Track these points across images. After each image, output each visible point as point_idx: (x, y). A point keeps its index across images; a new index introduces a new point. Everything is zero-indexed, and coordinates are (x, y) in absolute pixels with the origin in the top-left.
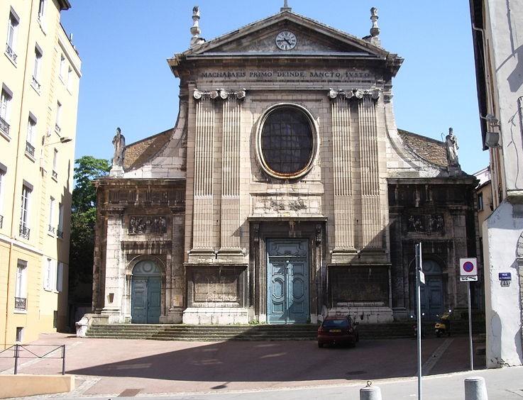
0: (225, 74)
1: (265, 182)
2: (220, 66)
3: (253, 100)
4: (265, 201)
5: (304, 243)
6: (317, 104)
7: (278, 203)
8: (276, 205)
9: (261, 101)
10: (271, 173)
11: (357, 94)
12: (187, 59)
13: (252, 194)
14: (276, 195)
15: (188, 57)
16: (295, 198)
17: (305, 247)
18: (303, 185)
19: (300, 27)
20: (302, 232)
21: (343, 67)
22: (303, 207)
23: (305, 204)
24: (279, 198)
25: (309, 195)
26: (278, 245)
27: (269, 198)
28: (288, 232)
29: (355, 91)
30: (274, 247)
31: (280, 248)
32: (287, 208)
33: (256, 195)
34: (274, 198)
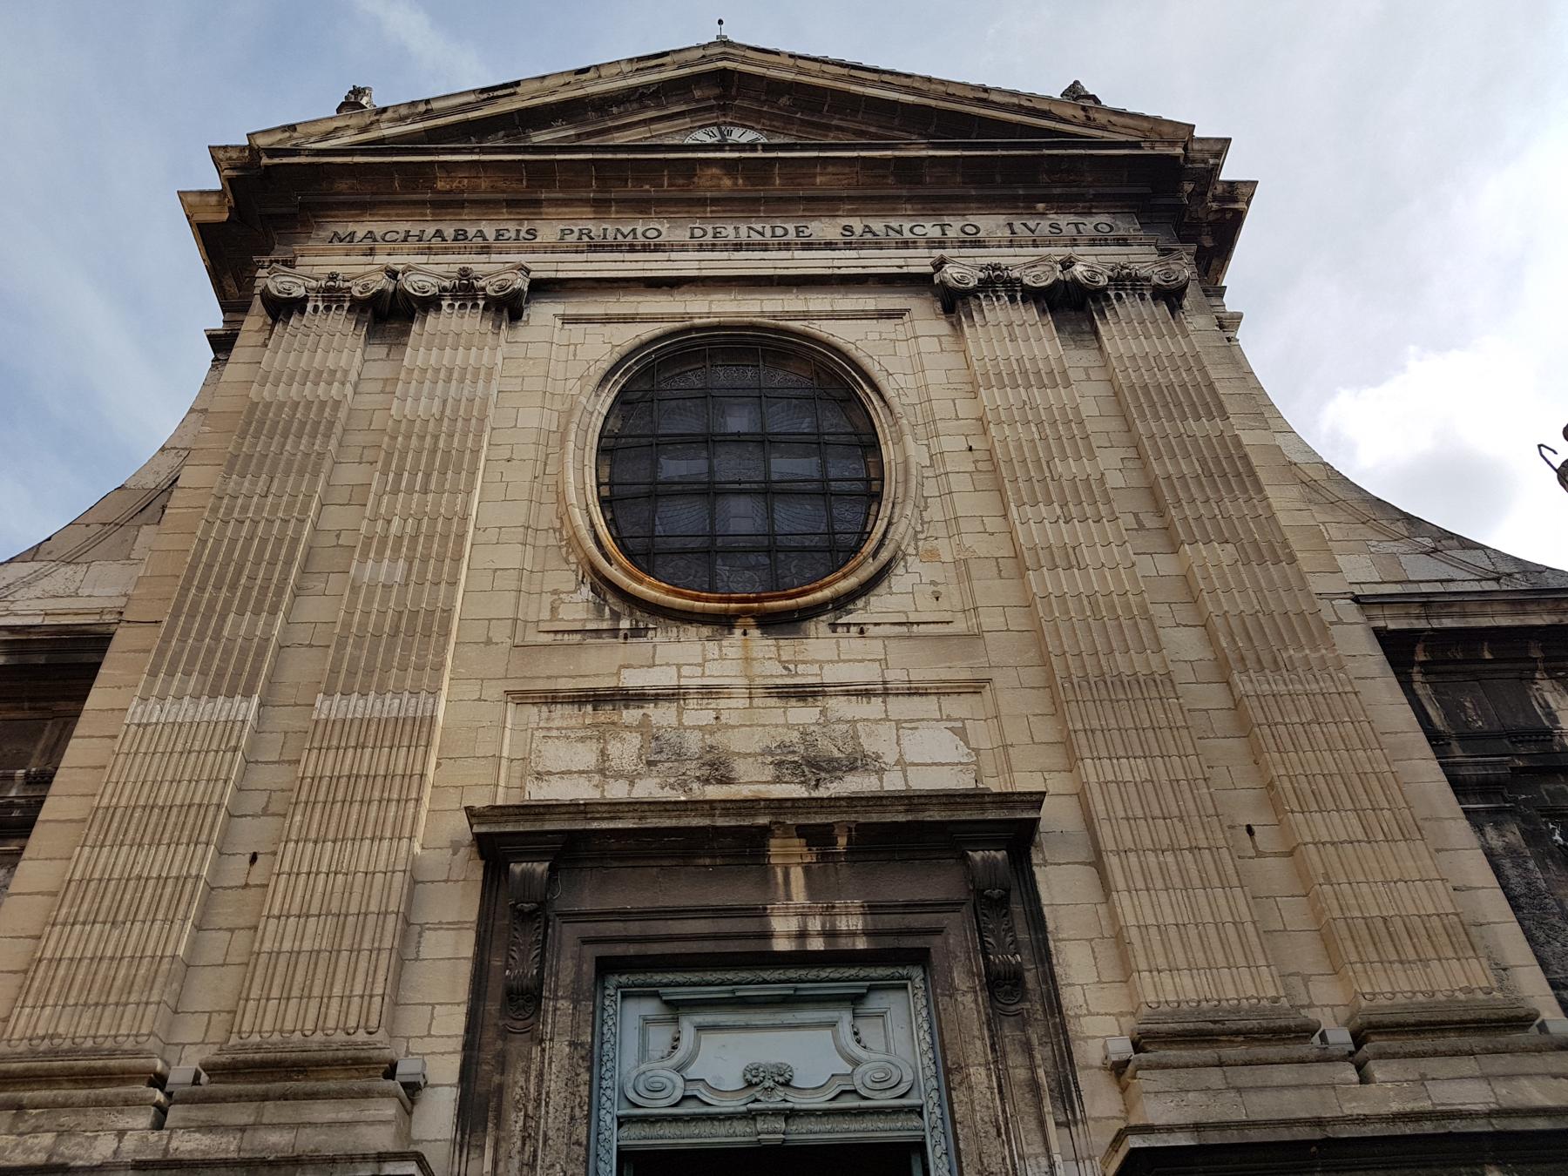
0: (439, 233)
1: (614, 632)
2: (423, 203)
3: (567, 320)
4: (601, 734)
5: (892, 1005)
6: (887, 326)
7: (693, 743)
8: (679, 756)
9: (608, 320)
10: (648, 590)
11: (1079, 270)
12: (265, 161)
13: (522, 698)
14: (675, 695)
15: (272, 152)
16: (804, 714)
17: (899, 1035)
18: (851, 645)
19: (784, 101)
20: (872, 909)
21: (990, 203)
22: (856, 763)
23: (869, 746)
24: (698, 714)
25: (886, 693)
26: (687, 1024)
27: (631, 715)
28: (760, 913)
29: (1067, 264)
30: (660, 1037)
31: (711, 1041)
32: (740, 767)
33: (552, 699)
34: (662, 715)
